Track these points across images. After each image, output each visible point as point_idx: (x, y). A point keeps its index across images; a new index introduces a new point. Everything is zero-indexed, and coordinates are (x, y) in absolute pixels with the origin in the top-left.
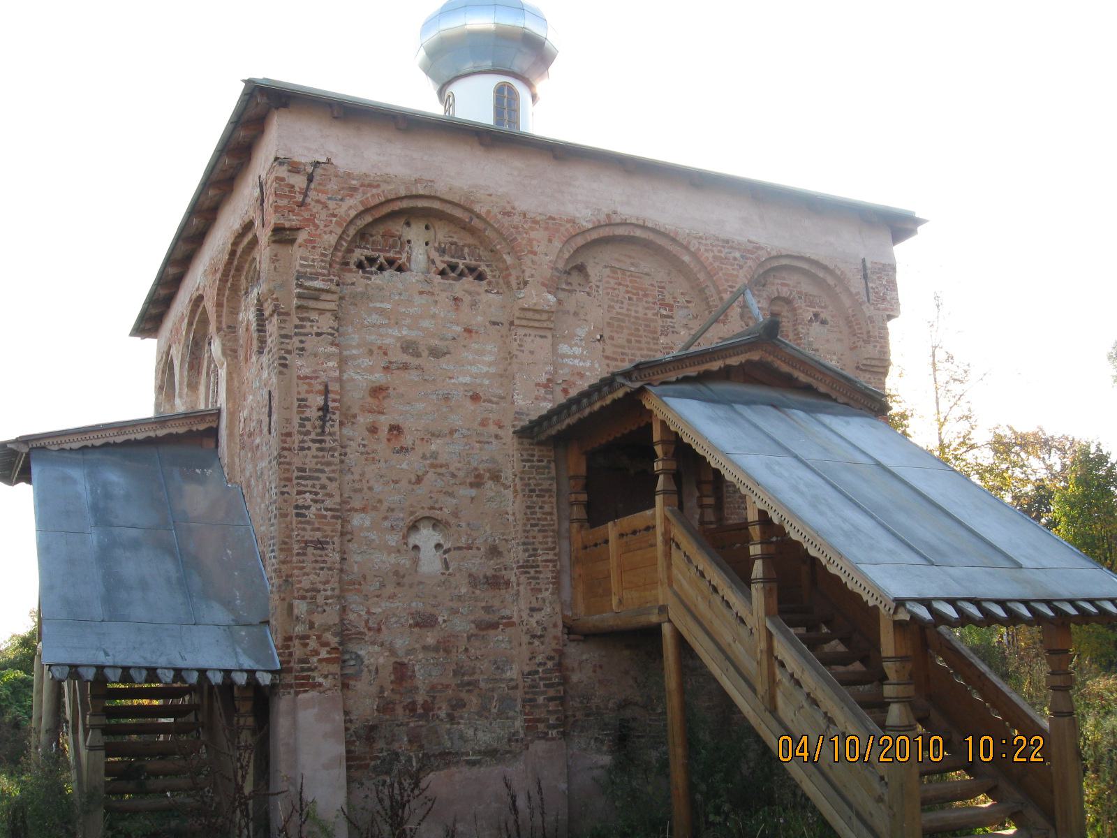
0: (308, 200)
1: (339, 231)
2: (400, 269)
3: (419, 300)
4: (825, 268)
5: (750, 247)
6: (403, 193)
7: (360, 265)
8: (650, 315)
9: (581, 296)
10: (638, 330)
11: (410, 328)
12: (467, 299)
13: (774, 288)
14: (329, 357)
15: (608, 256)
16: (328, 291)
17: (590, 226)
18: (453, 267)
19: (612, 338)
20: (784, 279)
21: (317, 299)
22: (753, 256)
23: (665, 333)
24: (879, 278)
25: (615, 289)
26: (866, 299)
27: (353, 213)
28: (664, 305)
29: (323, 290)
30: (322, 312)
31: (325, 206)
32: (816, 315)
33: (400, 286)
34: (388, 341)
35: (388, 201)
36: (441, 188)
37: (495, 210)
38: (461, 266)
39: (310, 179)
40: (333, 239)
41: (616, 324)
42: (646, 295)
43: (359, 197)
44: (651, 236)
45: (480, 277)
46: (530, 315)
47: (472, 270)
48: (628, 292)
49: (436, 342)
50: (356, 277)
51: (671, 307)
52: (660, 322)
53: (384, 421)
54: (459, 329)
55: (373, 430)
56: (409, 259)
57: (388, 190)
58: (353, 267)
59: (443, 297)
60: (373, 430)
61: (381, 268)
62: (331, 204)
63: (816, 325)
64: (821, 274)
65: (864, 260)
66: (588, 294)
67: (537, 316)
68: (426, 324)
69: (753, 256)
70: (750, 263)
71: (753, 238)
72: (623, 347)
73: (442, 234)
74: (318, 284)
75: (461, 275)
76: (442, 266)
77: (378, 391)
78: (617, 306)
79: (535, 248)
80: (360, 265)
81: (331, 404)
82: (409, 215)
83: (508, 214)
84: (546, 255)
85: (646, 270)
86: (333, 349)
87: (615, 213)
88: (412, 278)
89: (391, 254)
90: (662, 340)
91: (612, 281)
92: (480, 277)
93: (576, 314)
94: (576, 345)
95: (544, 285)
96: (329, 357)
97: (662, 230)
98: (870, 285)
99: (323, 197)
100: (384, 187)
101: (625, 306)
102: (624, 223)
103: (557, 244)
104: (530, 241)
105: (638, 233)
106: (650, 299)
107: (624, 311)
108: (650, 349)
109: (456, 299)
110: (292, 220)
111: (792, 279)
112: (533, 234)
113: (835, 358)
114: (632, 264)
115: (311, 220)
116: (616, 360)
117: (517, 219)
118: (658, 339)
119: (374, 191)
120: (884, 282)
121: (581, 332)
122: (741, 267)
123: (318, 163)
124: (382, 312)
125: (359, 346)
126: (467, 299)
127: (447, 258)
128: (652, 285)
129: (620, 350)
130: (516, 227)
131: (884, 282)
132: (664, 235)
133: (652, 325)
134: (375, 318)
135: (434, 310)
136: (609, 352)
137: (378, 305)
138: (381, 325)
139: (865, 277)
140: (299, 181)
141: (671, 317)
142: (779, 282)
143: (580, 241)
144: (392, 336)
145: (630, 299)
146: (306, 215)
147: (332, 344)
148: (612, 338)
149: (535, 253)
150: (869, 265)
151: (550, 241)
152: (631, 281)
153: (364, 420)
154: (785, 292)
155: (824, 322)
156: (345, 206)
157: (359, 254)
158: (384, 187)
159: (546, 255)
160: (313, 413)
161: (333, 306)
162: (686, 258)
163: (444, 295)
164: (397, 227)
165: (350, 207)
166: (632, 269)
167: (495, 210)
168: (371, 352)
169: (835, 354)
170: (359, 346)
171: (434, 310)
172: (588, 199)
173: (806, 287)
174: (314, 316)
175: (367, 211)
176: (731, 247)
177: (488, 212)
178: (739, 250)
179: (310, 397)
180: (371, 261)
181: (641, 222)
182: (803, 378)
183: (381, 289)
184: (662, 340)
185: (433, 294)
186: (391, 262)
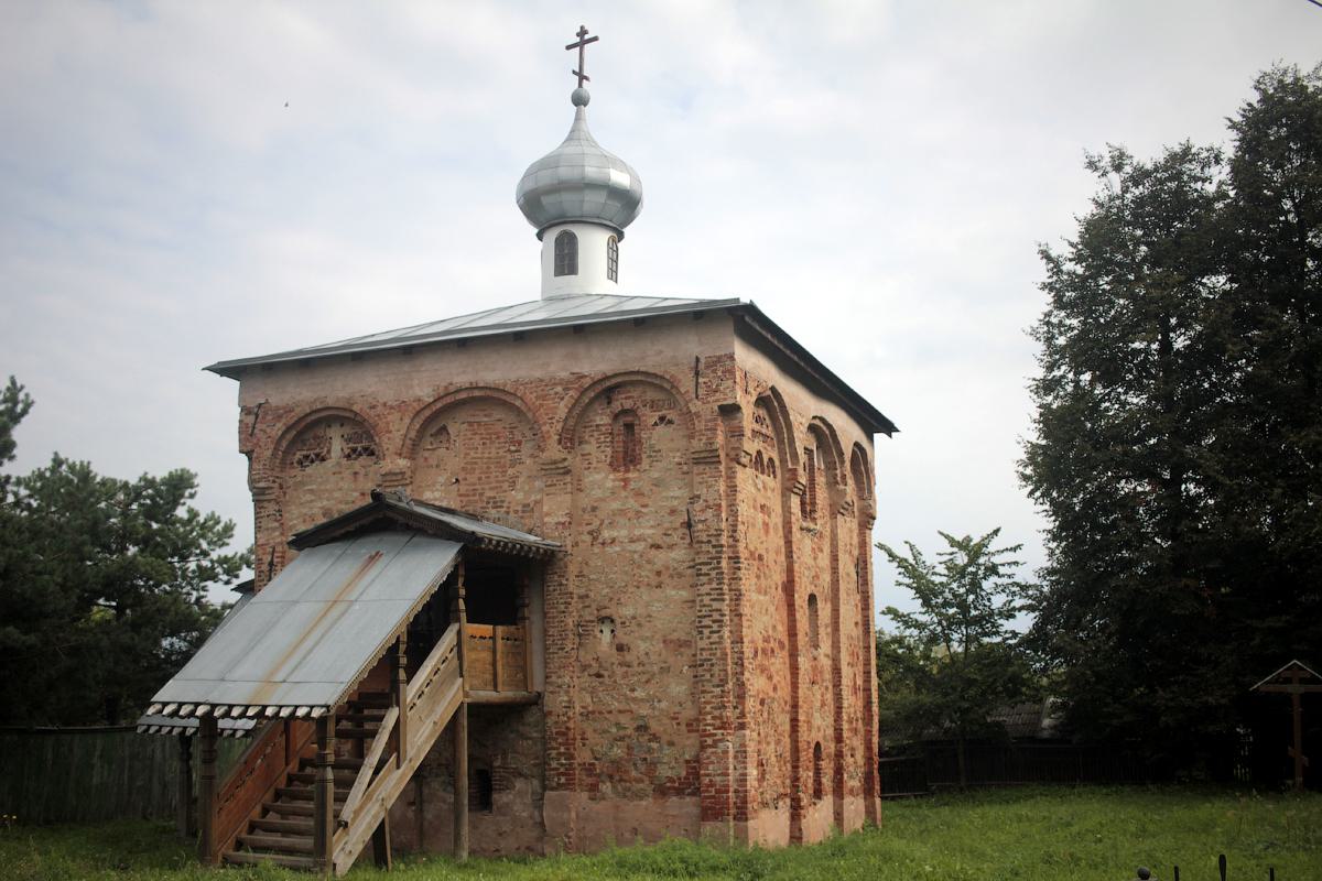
0: (256, 431)
1: (272, 447)
2: (323, 460)
3: (333, 479)
4: (655, 375)
5: (572, 378)
6: (308, 411)
7: (300, 462)
8: (501, 452)
9: (442, 451)
10: (488, 468)
11: (328, 500)
13: (618, 403)
14: (274, 529)
15: (463, 415)
16: (268, 488)
17: (431, 400)
18: (354, 450)
19: (465, 479)
20: (629, 392)
21: (264, 494)
22: (576, 386)
24: (714, 371)
25: (471, 439)
26: (694, 396)
27: (280, 433)
28: (513, 442)
29: (264, 488)
30: (269, 501)
31: (265, 432)
32: (662, 419)
33: (322, 471)
34: (315, 511)
35: (301, 419)
36: (330, 402)
37: (366, 407)
38: (359, 449)
39: (257, 416)
40: (268, 453)
41: (469, 467)
42: (498, 438)
43: (284, 420)
44: (489, 393)
45: (372, 454)
46: (388, 478)
47: (366, 449)
48: (482, 439)
50: (297, 471)
51: (520, 443)
52: (509, 456)
54: (356, 494)
56: (329, 452)
57: (299, 412)
58: (295, 465)
59: (347, 474)
61: (312, 462)
62: (268, 430)
63: (661, 428)
64: (657, 382)
65: (698, 360)
66: (447, 449)
67: (394, 478)
68: (337, 495)
69: (576, 386)
70: (571, 393)
71: (575, 371)
72: (475, 485)
73: (347, 430)
74: (262, 485)
75: (360, 455)
76: (347, 451)
78: (472, 454)
79: (391, 428)
80: (300, 462)
81: (275, 560)
83: (373, 407)
84: (398, 431)
85: (499, 417)
86: (277, 524)
87: (451, 384)
88: (329, 464)
89: (317, 451)
90: (510, 472)
91: (468, 433)
93: (437, 466)
94: (437, 490)
95: (396, 453)
96: (274, 529)
97: (493, 386)
98: (701, 380)
99: (264, 426)
100: (298, 410)
101: (480, 450)
102: (459, 391)
103: (407, 421)
104: (388, 423)
105: (477, 393)
106: (502, 440)
107: (479, 455)
108: (497, 482)
109: (356, 473)
111: (636, 393)
112: (390, 418)
113: (679, 454)
114: (486, 416)
116: (468, 495)
118: (506, 472)
119: (293, 414)
120: (720, 374)
121: (442, 479)
122: (562, 399)
123: (260, 404)
124: (311, 491)
125: (298, 518)
126: (363, 471)
127: (351, 445)
128: (505, 428)
129: (472, 488)
130: (378, 416)
131: (720, 374)
132: (496, 389)
133: (503, 461)
134: (309, 497)
135: (341, 484)
136: (461, 492)
137: (309, 487)
138: (312, 501)
139: (697, 374)
141: (519, 451)
142: (623, 396)
143: (427, 413)
145: (484, 444)
146: (255, 441)
147: (276, 520)
148: (465, 479)
149: (390, 432)
150: (703, 360)
151: (401, 419)
152: (485, 429)
154: (628, 404)
155: (670, 422)
156: (276, 428)
157: (299, 455)
158: (298, 410)
159: (395, 432)
161: (273, 497)
162: (518, 403)
163: (348, 472)
164: (320, 432)
166: (486, 419)
167: (366, 407)
168: (304, 521)
169: (678, 451)
170: (298, 518)
171: (341, 484)
172: (425, 383)
173: (651, 395)
174: (265, 504)
175: (288, 429)
176: (555, 384)
177: (361, 409)
178: (560, 384)
179: (264, 557)
180: (307, 457)
181: (474, 385)
182: (416, 525)
183: (310, 476)
184: (510, 472)
185: (340, 473)
186: (317, 455)
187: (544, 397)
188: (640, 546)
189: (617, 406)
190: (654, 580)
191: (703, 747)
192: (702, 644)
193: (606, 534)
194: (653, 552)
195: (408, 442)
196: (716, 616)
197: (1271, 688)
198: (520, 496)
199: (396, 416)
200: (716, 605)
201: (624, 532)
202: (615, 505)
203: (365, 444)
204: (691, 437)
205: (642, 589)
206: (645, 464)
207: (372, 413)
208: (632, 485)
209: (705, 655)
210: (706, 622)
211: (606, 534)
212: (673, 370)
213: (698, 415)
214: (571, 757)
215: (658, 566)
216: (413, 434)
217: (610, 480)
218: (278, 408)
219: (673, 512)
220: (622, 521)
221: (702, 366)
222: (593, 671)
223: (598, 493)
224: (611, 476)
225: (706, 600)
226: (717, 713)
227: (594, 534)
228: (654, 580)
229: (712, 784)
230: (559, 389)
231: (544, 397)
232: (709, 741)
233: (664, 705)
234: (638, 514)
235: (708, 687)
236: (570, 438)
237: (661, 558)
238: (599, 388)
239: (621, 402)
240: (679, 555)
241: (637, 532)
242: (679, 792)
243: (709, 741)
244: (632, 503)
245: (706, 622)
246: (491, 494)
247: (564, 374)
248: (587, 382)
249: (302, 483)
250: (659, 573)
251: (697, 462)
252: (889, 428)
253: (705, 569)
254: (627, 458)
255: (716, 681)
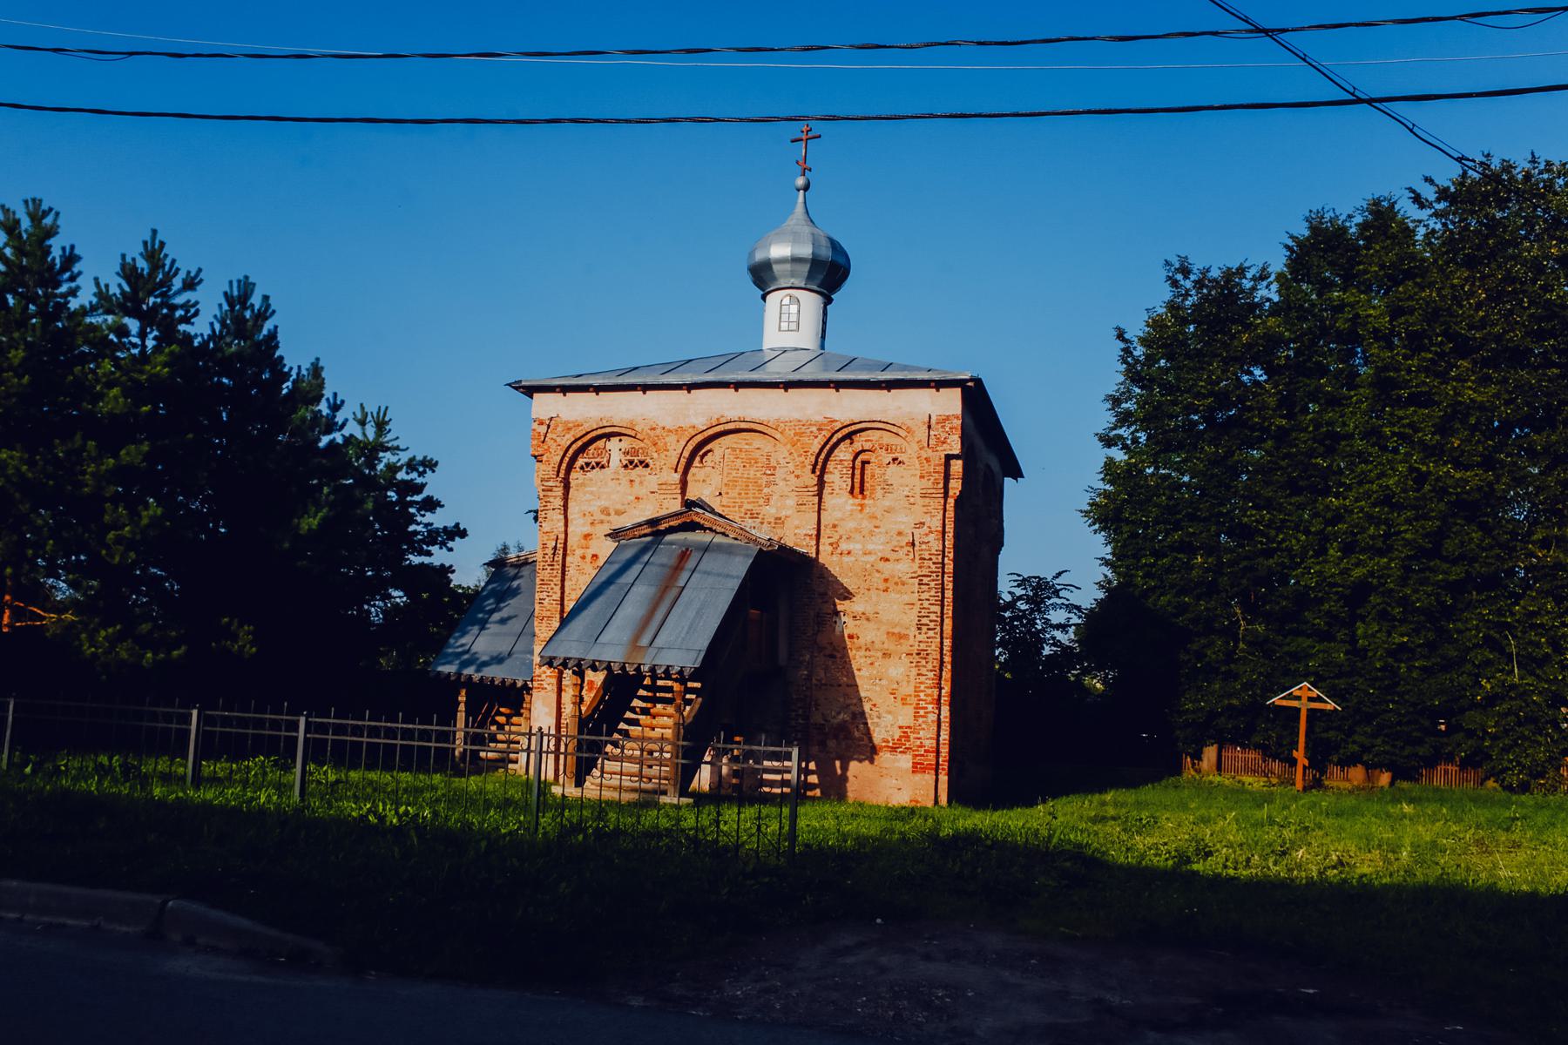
3: (611, 484)
12: (637, 480)
18: (631, 462)
23: (768, 486)
28: (769, 467)
45: (647, 466)
47: (641, 462)
49: (619, 507)
53: (589, 553)
55: (583, 558)
59: (625, 481)
60: (583, 558)
64: (895, 429)
73: (626, 443)
77: (587, 536)
82: (608, 436)
92: (647, 466)
110: (541, 451)
115: (547, 450)
117: (658, 432)
140: (543, 429)
143: (699, 438)
144: (595, 507)
153: (579, 552)
154: (867, 446)
159: (676, 448)
160: (550, 552)
164: (600, 443)
165: (569, 438)
173: (887, 438)
180: (588, 464)
187: (801, 434)
188: (871, 559)
189: (857, 446)
190: (882, 586)
191: (916, 718)
192: (922, 637)
193: (844, 546)
194: (881, 565)
195: (683, 461)
196: (933, 617)
197: (1284, 703)
198: (773, 511)
199: (671, 439)
200: (933, 608)
201: (858, 546)
202: (852, 525)
203: (641, 458)
204: (922, 477)
205: (873, 593)
206: (879, 493)
207: (652, 433)
208: (867, 510)
209: (923, 646)
210: (925, 621)
211: (844, 546)
212: (910, 423)
213: (928, 460)
214: (807, 718)
215: (886, 575)
216: (686, 454)
217: (850, 503)
218: (566, 422)
219: (900, 534)
220: (858, 537)
221: (933, 421)
222: (828, 652)
223: (839, 515)
224: (851, 501)
225: (926, 604)
226: (929, 691)
227: (835, 545)
228: (882, 586)
229: (921, 746)
230: (814, 429)
231: (801, 434)
232: (922, 712)
233: (884, 682)
234: (871, 534)
235: (923, 671)
236: (820, 468)
237: (887, 568)
238: (846, 431)
239: (860, 442)
240: (904, 567)
241: (870, 547)
242: (893, 749)
243: (922, 712)
244: (867, 525)
245: (925, 621)
246: (747, 506)
247: (819, 418)
248: (838, 426)
249: (583, 484)
250: (886, 580)
251: (924, 496)
252: (1017, 473)
253: (926, 580)
254: (859, 488)
255: (930, 666)
